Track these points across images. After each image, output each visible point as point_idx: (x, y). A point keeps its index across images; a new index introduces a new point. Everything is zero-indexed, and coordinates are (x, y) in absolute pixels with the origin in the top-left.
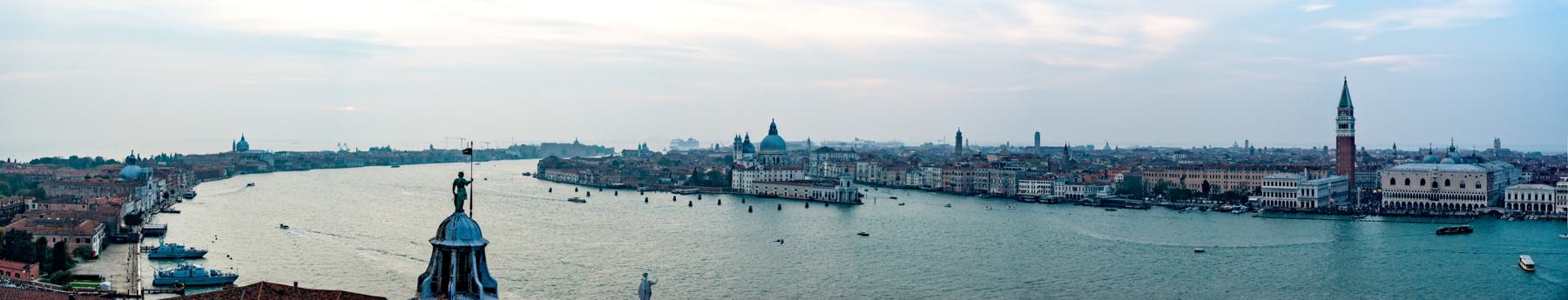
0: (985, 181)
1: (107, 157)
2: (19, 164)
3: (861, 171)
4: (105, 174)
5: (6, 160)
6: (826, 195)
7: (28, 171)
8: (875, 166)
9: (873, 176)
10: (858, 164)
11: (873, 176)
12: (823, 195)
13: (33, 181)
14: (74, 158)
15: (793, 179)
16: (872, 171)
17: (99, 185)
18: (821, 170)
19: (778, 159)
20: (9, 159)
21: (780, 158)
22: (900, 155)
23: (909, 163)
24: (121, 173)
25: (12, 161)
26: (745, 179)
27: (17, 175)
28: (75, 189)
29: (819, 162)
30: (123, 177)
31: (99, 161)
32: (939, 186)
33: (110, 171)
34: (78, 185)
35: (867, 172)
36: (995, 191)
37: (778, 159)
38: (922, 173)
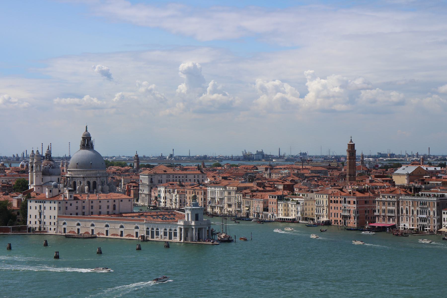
0: (391, 211)
3: (213, 199)
6: (165, 234)
8: (233, 194)
9: (230, 206)
10: (209, 189)
11: (230, 206)
12: (162, 233)
15: (117, 211)
16: (229, 199)
18: (156, 198)
19: (95, 183)
21: (98, 182)
22: (266, 176)
23: (281, 187)
26: (47, 213)
29: (152, 185)
32: (325, 219)
35: (222, 199)
36: (408, 226)
37: (95, 183)
38: (301, 201)
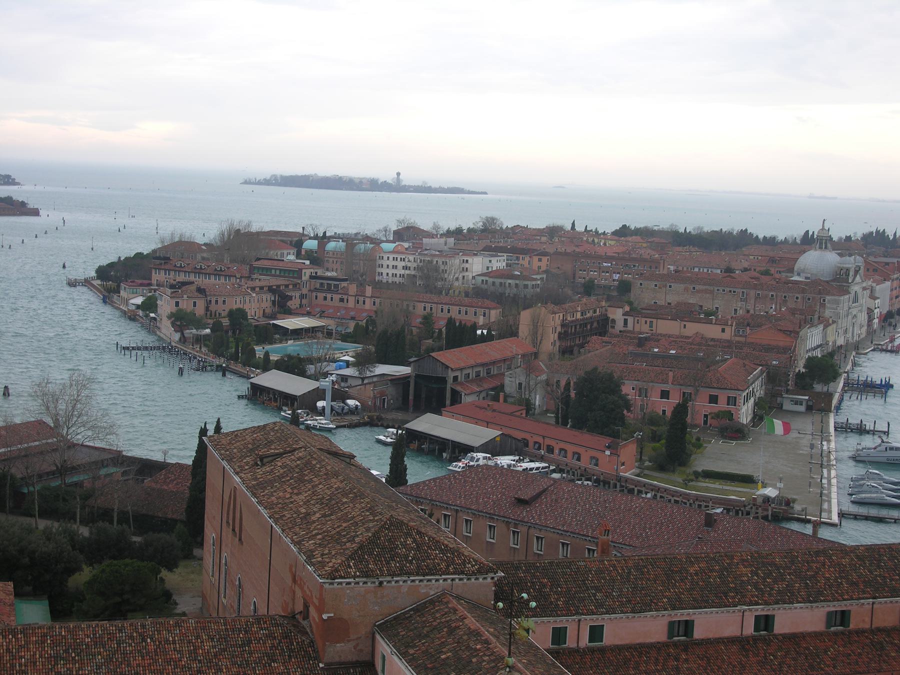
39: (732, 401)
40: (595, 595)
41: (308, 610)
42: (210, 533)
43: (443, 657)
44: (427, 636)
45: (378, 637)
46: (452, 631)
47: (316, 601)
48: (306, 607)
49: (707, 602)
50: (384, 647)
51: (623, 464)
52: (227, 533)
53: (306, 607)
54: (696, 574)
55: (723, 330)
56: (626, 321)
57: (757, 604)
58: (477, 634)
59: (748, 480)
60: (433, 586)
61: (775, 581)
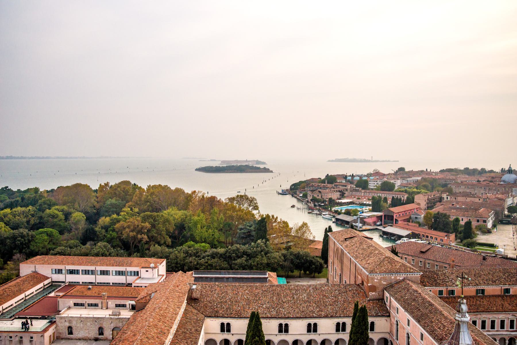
1: (488, 168)
2: (433, 172)
4: (490, 179)
5: (425, 170)
7: (440, 176)
13: (444, 183)
14: (467, 169)
17: (488, 186)
20: (427, 170)
24: (502, 179)
25: (429, 170)
27: (434, 179)
28: (472, 188)
30: (504, 181)
31: (483, 171)
33: (493, 178)
34: (473, 186)
39: (485, 221)
40: (451, 281)
41: (363, 283)
42: (330, 260)
43: (406, 298)
44: (400, 291)
45: (385, 291)
46: (408, 290)
47: (366, 281)
48: (363, 282)
49: (489, 283)
50: (387, 294)
51: (451, 241)
52: (336, 261)
53: (363, 282)
54: (484, 275)
55: (479, 200)
56: (447, 198)
57: (506, 285)
58: (417, 291)
59: (492, 246)
60: (400, 277)
61: (512, 277)
